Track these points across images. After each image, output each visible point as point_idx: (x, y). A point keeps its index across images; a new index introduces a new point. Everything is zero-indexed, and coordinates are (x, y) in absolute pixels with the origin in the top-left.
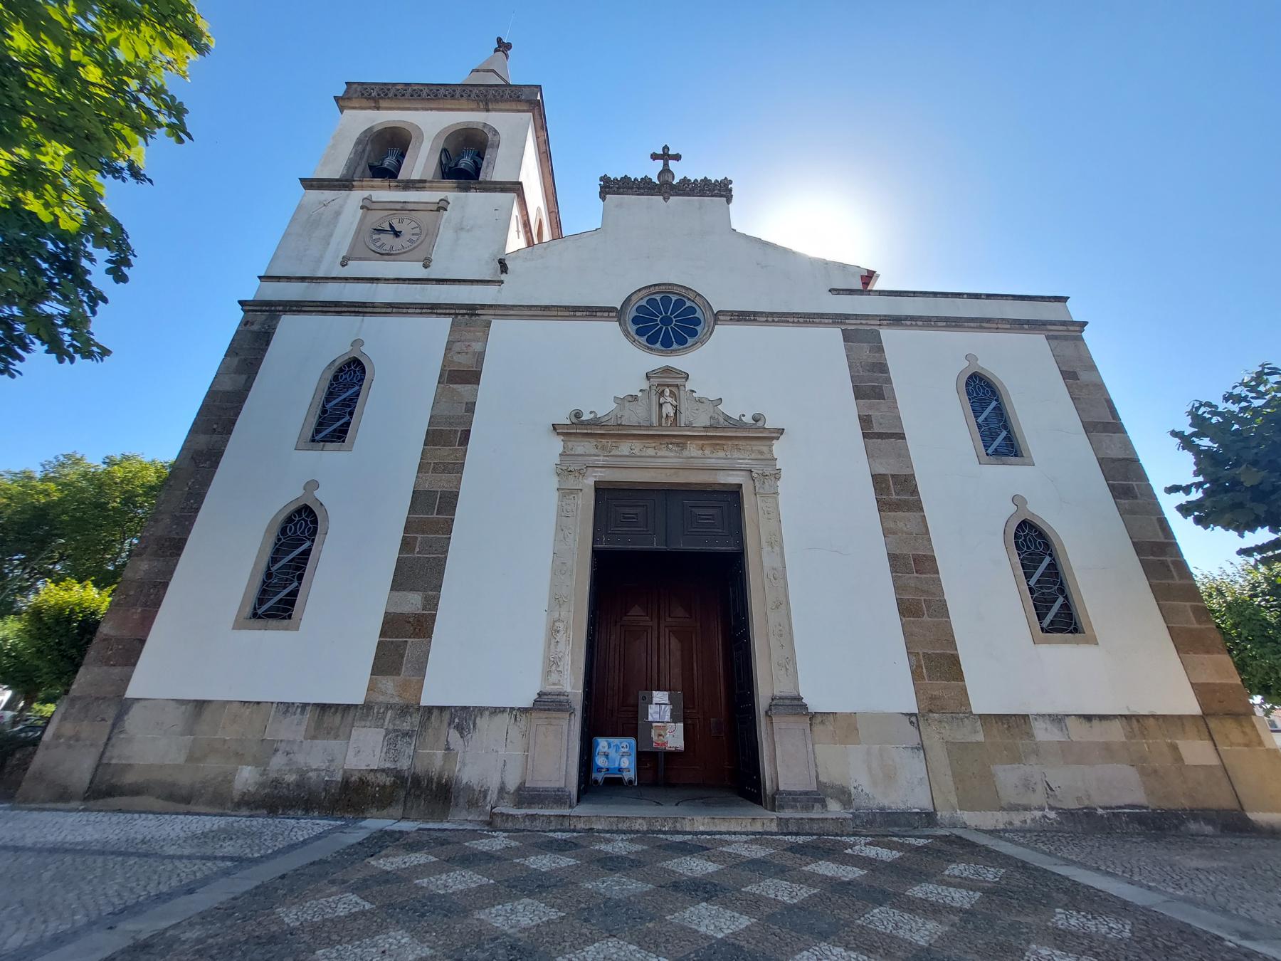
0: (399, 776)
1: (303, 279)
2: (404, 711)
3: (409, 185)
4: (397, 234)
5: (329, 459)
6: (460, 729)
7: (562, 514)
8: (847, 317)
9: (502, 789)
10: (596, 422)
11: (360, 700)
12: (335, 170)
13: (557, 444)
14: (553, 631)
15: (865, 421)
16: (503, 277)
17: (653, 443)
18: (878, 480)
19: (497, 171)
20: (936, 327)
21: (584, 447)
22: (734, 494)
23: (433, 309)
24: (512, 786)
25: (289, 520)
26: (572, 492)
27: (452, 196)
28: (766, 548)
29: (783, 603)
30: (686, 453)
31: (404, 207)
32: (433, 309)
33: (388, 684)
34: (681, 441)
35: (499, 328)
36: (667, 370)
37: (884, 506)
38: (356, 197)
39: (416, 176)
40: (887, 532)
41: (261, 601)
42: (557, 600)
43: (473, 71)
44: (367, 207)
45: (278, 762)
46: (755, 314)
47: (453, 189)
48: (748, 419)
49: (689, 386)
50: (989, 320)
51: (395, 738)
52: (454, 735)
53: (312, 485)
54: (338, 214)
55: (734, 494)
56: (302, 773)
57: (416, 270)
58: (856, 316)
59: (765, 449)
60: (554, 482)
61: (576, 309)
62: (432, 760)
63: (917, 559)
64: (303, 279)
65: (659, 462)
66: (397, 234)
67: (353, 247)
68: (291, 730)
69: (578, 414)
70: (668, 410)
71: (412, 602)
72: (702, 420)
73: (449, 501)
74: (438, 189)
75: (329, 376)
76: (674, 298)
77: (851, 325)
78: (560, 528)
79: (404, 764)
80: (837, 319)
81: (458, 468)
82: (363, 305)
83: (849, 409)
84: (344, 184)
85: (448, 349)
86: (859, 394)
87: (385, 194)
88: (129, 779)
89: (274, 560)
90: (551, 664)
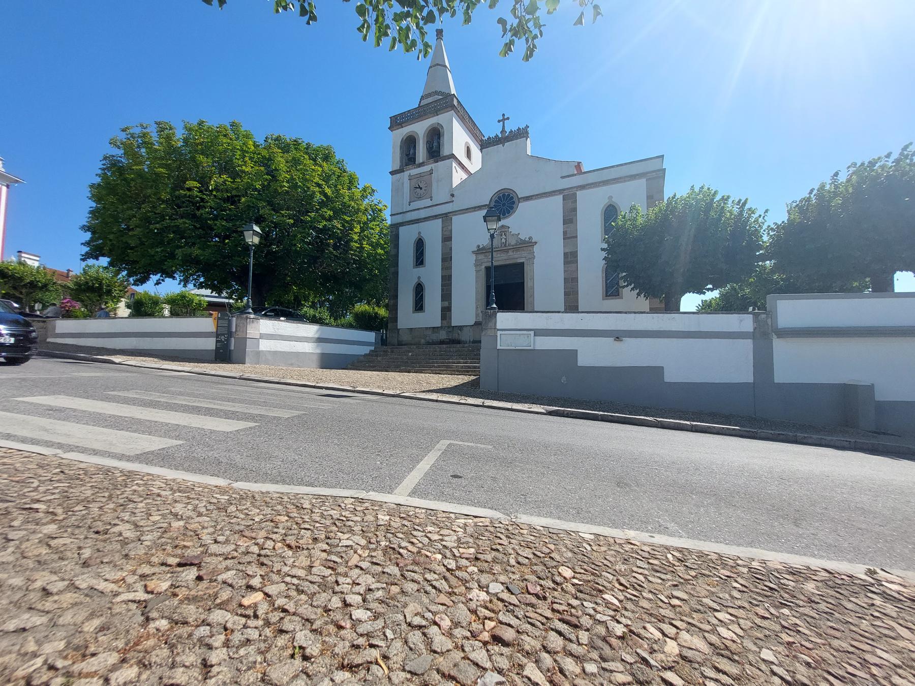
0: (449, 339)
1: (401, 213)
2: (449, 327)
3: (421, 165)
4: (421, 189)
5: (421, 271)
6: (460, 330)
7: (477, 277)
8: (564, 190)
9: (470, 341)
10: (484, 248)
11: (440, 326)
12: (397, 167)
13: (474, 257)
14: (477, 308)
15: (565, 233)
16: (454, 199)
17: (499, 252)
18: (566, 255)
19: (445, 152)
20: (599, 186)
21: (481, 257)
22: (522, 265)
23: (436, 217)
24: (472, 340)
25: (417, 287)
26: (478, 271)
27: (433, 165)
28: (529, 280)
29: (533, 295)
30: (509, 254)
31: (420, 176)
32: (436, 217)
33: (445, 322)
34: (507, 251)
35: (455, 219)
36: (503, 226)
37: (566, 263)
38: (406, 173)
39: (421, 161)
40: (565, 271)
41: (416, 307)
42: (477, 300)
43: (430, 67)
44: (411, 178)
45: (428, 338)
46: (532, 196)
47: (433, 163)
48: (527, 239)
49: (510, 230)
50: (620, 178)
51: (448, 332)
52: (459, 331)
53: (419, 278)
54: (403, 184)
55: (522, 265)
56: (432, 340)
57: (427, 202)
58: (568, 189)
59: (531, 249)
60: (474, 268)
61: (475, 207)
62: (455, 336)
63: (572, 279)
64: (401, 213)
65: (500, 259)
66: (421, 189)
67: (410, 198)
68: (429, 332)
69: (478, 246)
70: (504, 240)
71: (446, 303)
72: (513, 242)
73: (450, 277)
74: (429, 164)
75: (415, 245)
76: (506, 194)
77: (566, 193)
78: (476, 282)
79: (450, 337)
80: (560, 192)
81: (451, 268)
82: (418, 220)
83: (560, 228)
84: (400, 171)
85: (442, 230)
86: (565, 222)
87: (415, 171)
88: (404, 343)
89: (416, 297)
90: (477, 315)
